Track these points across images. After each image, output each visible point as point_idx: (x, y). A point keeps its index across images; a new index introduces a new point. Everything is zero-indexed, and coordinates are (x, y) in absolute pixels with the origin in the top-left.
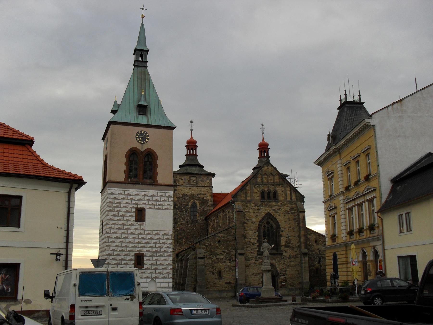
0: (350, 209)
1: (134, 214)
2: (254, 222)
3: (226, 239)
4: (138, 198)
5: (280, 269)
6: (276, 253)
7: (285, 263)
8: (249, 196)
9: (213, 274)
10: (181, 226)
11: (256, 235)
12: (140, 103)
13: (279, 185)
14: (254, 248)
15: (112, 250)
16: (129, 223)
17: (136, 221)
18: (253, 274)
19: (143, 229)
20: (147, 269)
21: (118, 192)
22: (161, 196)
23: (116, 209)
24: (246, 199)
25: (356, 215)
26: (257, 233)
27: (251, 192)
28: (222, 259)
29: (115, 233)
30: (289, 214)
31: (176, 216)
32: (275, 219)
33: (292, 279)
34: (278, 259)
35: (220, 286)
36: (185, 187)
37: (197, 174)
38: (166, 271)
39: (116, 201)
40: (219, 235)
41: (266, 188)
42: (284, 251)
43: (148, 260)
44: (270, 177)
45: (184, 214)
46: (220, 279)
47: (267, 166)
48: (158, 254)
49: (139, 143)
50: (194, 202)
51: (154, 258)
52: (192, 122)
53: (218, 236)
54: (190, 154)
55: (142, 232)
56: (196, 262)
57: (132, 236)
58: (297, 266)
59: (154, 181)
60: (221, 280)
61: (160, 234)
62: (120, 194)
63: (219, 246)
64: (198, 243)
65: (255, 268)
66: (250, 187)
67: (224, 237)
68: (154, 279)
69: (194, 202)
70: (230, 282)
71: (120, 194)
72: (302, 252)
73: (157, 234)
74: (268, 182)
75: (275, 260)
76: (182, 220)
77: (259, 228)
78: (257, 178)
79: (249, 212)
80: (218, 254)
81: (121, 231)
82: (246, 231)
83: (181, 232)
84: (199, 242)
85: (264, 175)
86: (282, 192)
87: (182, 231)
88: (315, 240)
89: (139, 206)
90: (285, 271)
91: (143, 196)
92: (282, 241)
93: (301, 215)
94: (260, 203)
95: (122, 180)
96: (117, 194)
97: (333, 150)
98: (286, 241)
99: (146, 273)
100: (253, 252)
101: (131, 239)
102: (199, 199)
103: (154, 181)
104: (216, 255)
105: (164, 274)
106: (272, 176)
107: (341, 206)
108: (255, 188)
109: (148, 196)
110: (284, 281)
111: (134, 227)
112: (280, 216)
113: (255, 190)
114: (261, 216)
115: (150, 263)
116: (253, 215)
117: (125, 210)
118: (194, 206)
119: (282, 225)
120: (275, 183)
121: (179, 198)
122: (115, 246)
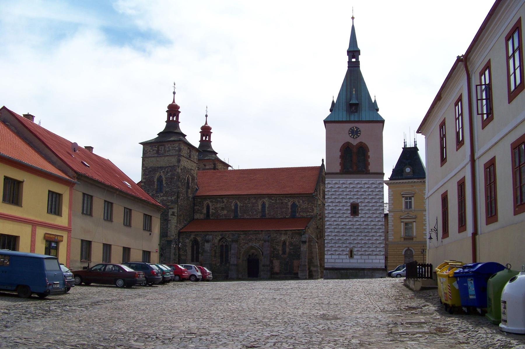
36: (185, 159)
76: (182, 195)
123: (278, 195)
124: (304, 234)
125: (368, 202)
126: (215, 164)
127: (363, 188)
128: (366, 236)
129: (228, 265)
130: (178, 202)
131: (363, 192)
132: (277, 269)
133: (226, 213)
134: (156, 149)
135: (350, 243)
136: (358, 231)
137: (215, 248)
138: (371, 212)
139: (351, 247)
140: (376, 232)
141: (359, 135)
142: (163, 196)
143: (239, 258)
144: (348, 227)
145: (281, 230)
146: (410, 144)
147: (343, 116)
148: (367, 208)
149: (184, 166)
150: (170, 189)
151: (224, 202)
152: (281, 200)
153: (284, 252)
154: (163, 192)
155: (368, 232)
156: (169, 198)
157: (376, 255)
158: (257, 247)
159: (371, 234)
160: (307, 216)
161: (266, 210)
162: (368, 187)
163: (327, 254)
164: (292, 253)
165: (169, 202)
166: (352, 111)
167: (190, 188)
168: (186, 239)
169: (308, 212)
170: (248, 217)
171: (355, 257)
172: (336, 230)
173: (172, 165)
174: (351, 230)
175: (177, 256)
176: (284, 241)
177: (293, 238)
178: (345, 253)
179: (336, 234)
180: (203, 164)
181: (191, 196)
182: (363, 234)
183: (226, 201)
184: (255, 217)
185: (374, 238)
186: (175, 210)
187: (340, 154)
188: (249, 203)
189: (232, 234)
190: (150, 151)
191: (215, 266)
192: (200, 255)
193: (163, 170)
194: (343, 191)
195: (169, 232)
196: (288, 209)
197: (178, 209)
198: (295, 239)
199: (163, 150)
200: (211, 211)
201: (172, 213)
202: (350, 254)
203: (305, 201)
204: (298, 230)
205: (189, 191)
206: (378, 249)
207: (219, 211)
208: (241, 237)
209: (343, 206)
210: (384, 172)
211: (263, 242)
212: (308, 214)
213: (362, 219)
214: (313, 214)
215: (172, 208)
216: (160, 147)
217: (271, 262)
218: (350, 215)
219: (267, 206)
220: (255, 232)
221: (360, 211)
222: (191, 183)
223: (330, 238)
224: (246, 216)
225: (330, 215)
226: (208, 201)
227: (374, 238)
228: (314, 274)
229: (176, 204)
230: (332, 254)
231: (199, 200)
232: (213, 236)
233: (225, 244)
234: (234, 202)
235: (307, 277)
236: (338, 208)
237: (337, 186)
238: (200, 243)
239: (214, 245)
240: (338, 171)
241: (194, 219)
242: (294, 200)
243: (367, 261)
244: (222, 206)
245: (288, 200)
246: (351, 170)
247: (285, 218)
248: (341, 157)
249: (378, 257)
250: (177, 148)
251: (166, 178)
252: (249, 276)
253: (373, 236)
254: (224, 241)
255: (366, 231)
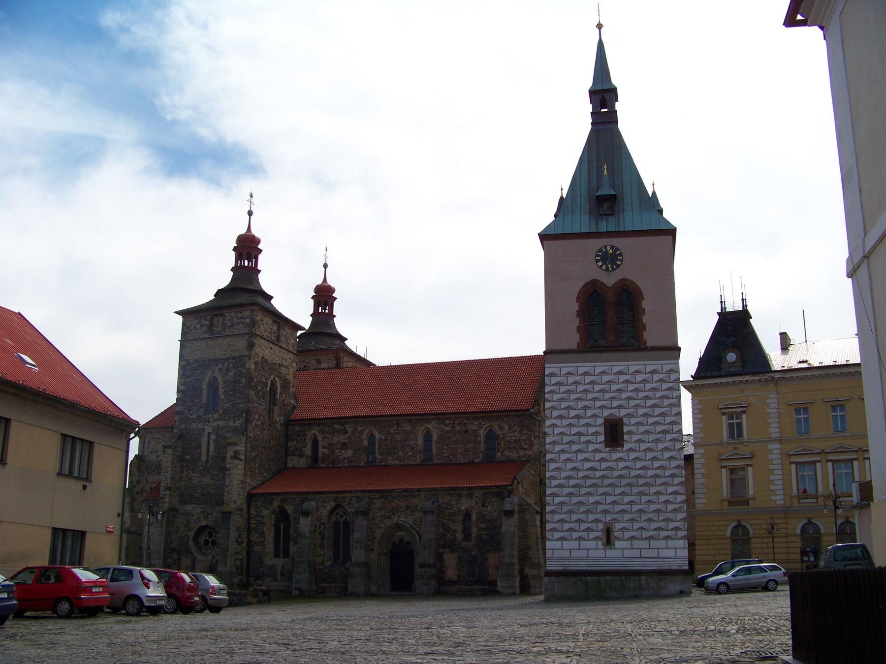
36: (266, 343)
76: (257, 417)
123: (458, 416)
124: (508, 496)
125: (645, 415)
126: (338, 359)
127: (632, 383)
128: (641, 493)
129: (348, 564)
130: (246, 431)
131: (632, 391)
132: (451, 573)
133: (351, 455)
134: (208, 323)
135: (605, 512)
136: (624, 482)
137: (322, 527)
138: (652, 437)
139: (607, 520)
140: (664, 484)
141: (619, 263)
142: (219, 419)
143: (372, 550)
144: (598, 474)
145: (460, 489)
146: (732, 305)
147: (582, 223)
148: (642, 429)
149: (263, 357)
150: (232, 405)
151: (346, 433)
152: (464, 425)
153: (467, 536)
154: (217, 411)
155: (646, 484)
156: (231, 424)
157: (667, 538)
158: (409, 526)
159: (653, 490)
160: (519, 457)
161: (434, 448)
162: (644, 381)
163: (550, 537)
164: (484, 536)
165: (229, 432)
166: (601, 212)
167: (279, 404)
168: (263, 508)
169: (522, 448)
170: (396, 462)
171: (618, 544)
172: (572, 482)
173: (237, 354)
174: (607, 482)
175: (245, 545)
176: (467, 512)
177: (487, 504)
178: (593, 535)
179: (571, 490)
180: (316, 360)
181: (279, 419)
182: (635, 490)
183: (351, 429)
184: (411, 462)
185: (662, 498)
186: (241, 448)
187: (575, 307)
188: (398, 434)
189: (357, 497)
190: (195, 327)
191: (322, 567)
192: (291, 543)
193: (220, 366)
194: (585, 391)
195: (226, 494)
196: (480, 442)
197: (248, 446)
198: (489, 508)
199: (220, 325)
200: (321, 450)
201: (232, 454)
202: (605, 539)
203: (514, 425)
204: (497, 487)
205: (276, 409)
206: (672, 525)
207: (336, 451)
208: (375, 504)
209: (587, 425)
210: (679, 345)
211: (421, 514)
212: (521, 454)
213: (632, 455)
214: (530, 453)
215: (235, 444)
216: (216, 319)
217: (440, 557)
218: (603, 445)
219: (435, 438)
220: (405, 493)
221: (626, 437)
222: (281, 393)
223: (557, 500)
224: (391, 461)
225: (558, 448)
226: (315, 431)
227: (662, 498)
228: (532, 583)
229: (243, 435)
230: (562, 539)
231: (297, 429)
232: (317, 503)
233: (344, 519)
234: (368, 430)
235: (518, 591)
236: (574, 430)
237: (571, 379)
238: (292, 517)
239: (319, 520)
240: (575, 346)
241: (286, 468)
242: (492, 424)
243: (645, 553)
244: (343, 441)
245: (479, 424)
246: (603, 342)
247: (472, 463)
248: (579, 314)
249: (671, 543)
250: (248, 320)
251: (225, 382)
252: (393, 589)
253: (658, 493)
254: (341, 512)
255: (641, 481)
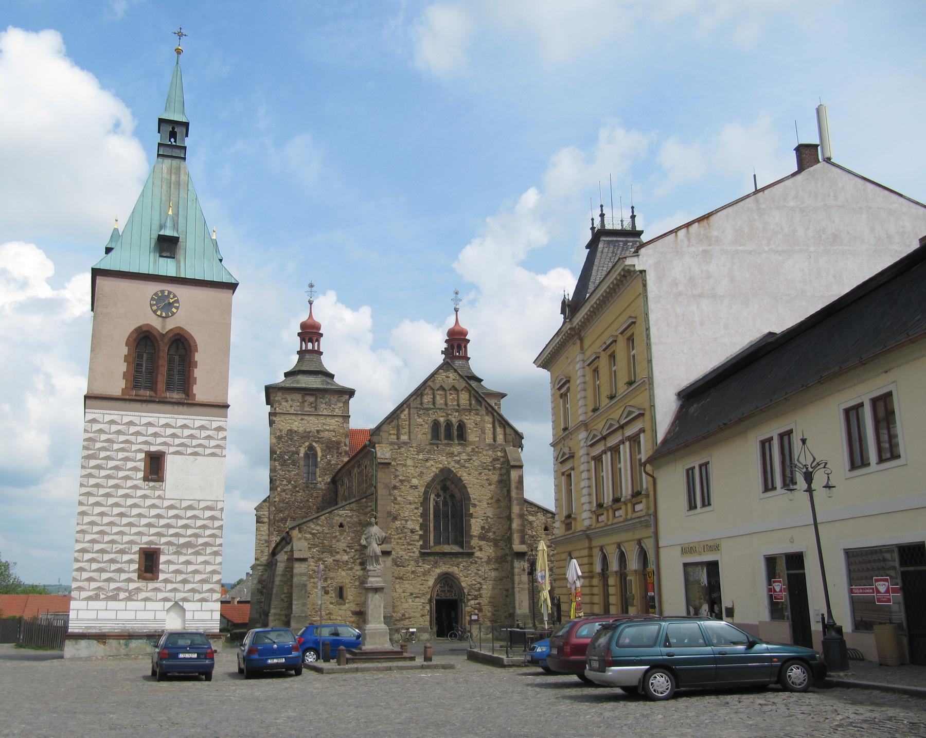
0: (598, 459)
1: (141, 465)
2: (416, 487)
3: (355, 520)
4: (151, 430)
5: (469, 586)
6: (461, 551)
7: (480, 572)
8: (405, 433)
9: (327, 592)
10: (283, 494)
11: (419, 514)
12: (162, 233)
13: (470, 411)
14: (414, 541)
15: (89, 542)
16: (130, 483)
17: (146, 479)
18: (412, 594)
19: (159, 497)
20: (166, 581)
21: (108, 418)
22: (202, 428)
23: (103, 454)
24: (398, 438)
25: (607, 471)
26: (421, 510)
27: (409, 425)
28: (347, 561)
29: (98, 504)
30: (489, 470)
31: (274, 474)
32: (460, 480)
33: (496, 607)
34: (464, 564)
35: (340, 618)
36: (294, 417)
37: (317, 390)
38: (206, 587)
39: (104, 437)
40: (341, 512)
41: (442, 417)
42: (477, 548)
43: (169, 562)
44: (451, 394)
45: (288, 471)
46: (341, 604)
47: (446, 371)
48: (190, 551)
49: (156, 317)
50: (311, 448)
51: (182, 559)
52: (311, 286)
53: (339, 515)
54: (307, 351)
55: (156, 502)
56: (292, 568)
57: (135, 511)
58: (505, 579)
59: (187, 395)
60: (343, 607)
61: (197, 506)
62: (112, 422)
63: (341, 535)
64: (297, 529)
65: (413, 582)
66: (409, 414)
67: (351, 517)
68: (181, 603)
69: (311, 448)
70: (362, 610)
71: (112, 422)
72: (515, 551)
73: (190, 508)
74: (446, 404)
75: (458, 565)
76: (285, 482)
77: (426, 499)
78: (422, 395)
79: (405, 465)
80: (338, 553)
81: (111, 501)
82: (399, 504)
83: (282, 507)
84: (298, 525)
85: (438, 390)
86: (476, 424)
87: (285, 505)
88: (543, 527)
89: (153, 449)
90: (479, 589)
91: (162, 426)
92: (473, 527)
93: (514, 474)
94: (428, 447)
95: (117, 392)
96: (105, 421)
97: (567, 332)
98: (483, 528)
99: (164, 589)
100: (412, 549)
101: (133, 517)
102: (321, 440)
103: (187, 395)
104: (334, 554)
105: (202, 593)
106: (456, 392)
107: (582, 452)
108: (418, 416)
109: (174, 428)
110: (476, 611)
111: (140, 493)
112: (469, 474)
113: (420, 420)
114: (430, 474)
115: (172, 568)
116: (412, 472)
117: (121, 455)
118: (311, 454)
119: (474, 492)
120: (462, 407)
121: (279, 438)
122: (97, 533)
